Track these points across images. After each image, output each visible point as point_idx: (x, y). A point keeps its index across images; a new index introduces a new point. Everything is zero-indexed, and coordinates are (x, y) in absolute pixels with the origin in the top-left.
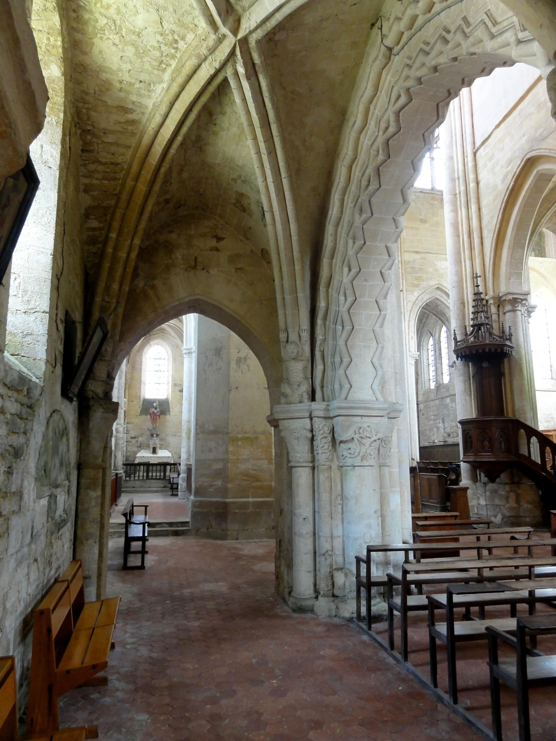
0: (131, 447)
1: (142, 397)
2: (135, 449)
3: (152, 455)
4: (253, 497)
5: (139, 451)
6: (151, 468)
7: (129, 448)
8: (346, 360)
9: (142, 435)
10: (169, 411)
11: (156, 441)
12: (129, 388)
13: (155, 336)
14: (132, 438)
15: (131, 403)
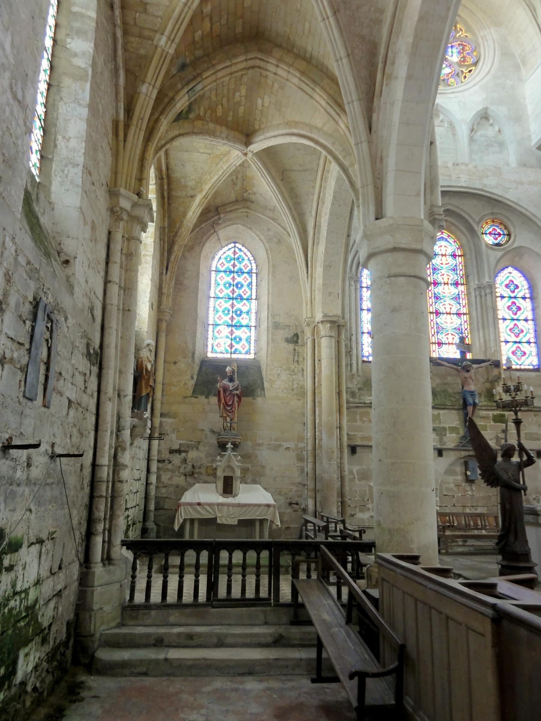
0: (169, 475)
1: (197, 354)
2: (180, 480)
3: (221, 500)
5: (191, 485)
6: (224, 555)
7: (165, 478)
9: (196, 446)
10: (263, 389)
11: (233, 461)
12: (168, 332)
13: (229, 216)
14: (172, 452)
15: (173, 367)
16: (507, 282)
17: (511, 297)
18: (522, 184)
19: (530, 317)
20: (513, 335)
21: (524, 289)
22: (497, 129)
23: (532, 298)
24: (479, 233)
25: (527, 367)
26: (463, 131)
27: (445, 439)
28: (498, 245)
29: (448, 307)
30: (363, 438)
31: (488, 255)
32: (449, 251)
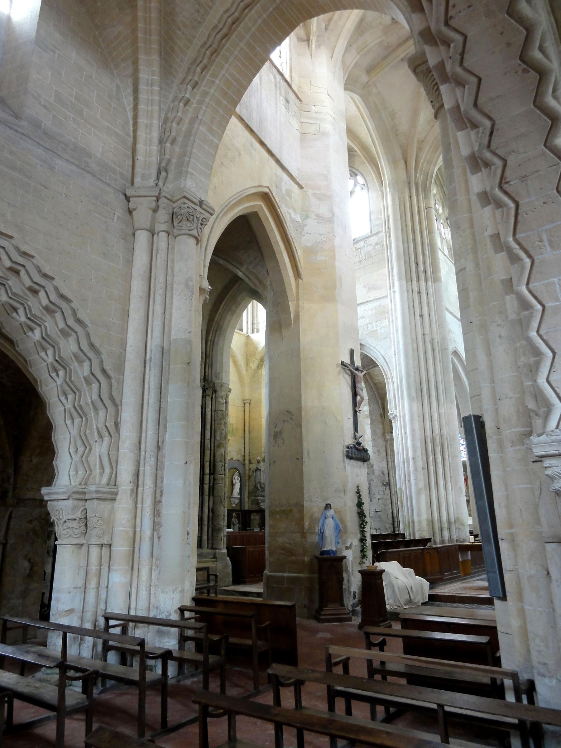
4: (289, 572)
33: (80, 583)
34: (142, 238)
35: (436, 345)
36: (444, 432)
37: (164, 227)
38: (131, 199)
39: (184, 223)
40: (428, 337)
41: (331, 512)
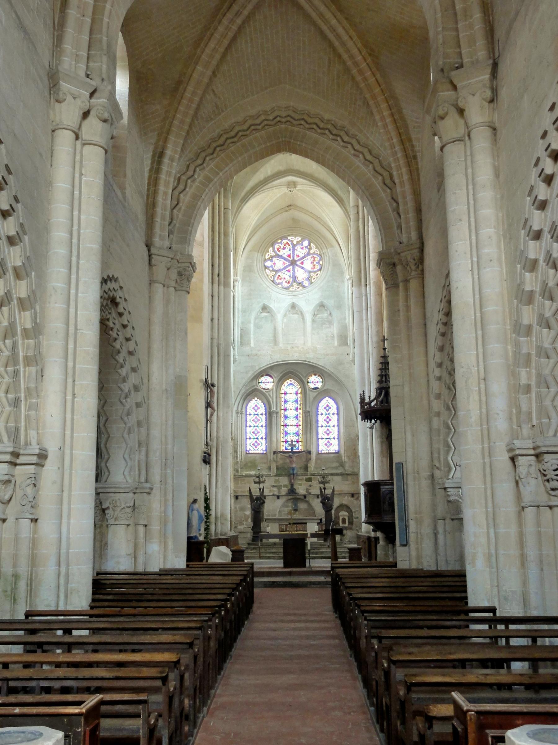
8: (106, 457)
16: (325, 406)
17: (326, 414)
18: (327, 355)
19: (336, 424)
20: (326, 435)
21: (334, 409)
22: (329, 312)
23: (338, 414)
24: (306, 383)
25: (332, 451)
26: (309, 318)
27: (281, 491)
28: (317, 388)
29: (291, 422)
30: (242, 492)
31: (309, 395)
32: (295, 390)
33: (131, 551)
34: (159, 289)
35: (222, 351)
36: (221, 434)
37: (173, 283)
38: (153, 256)
39: (185, 281)
40: (215, 342)
41: (196, 506)
